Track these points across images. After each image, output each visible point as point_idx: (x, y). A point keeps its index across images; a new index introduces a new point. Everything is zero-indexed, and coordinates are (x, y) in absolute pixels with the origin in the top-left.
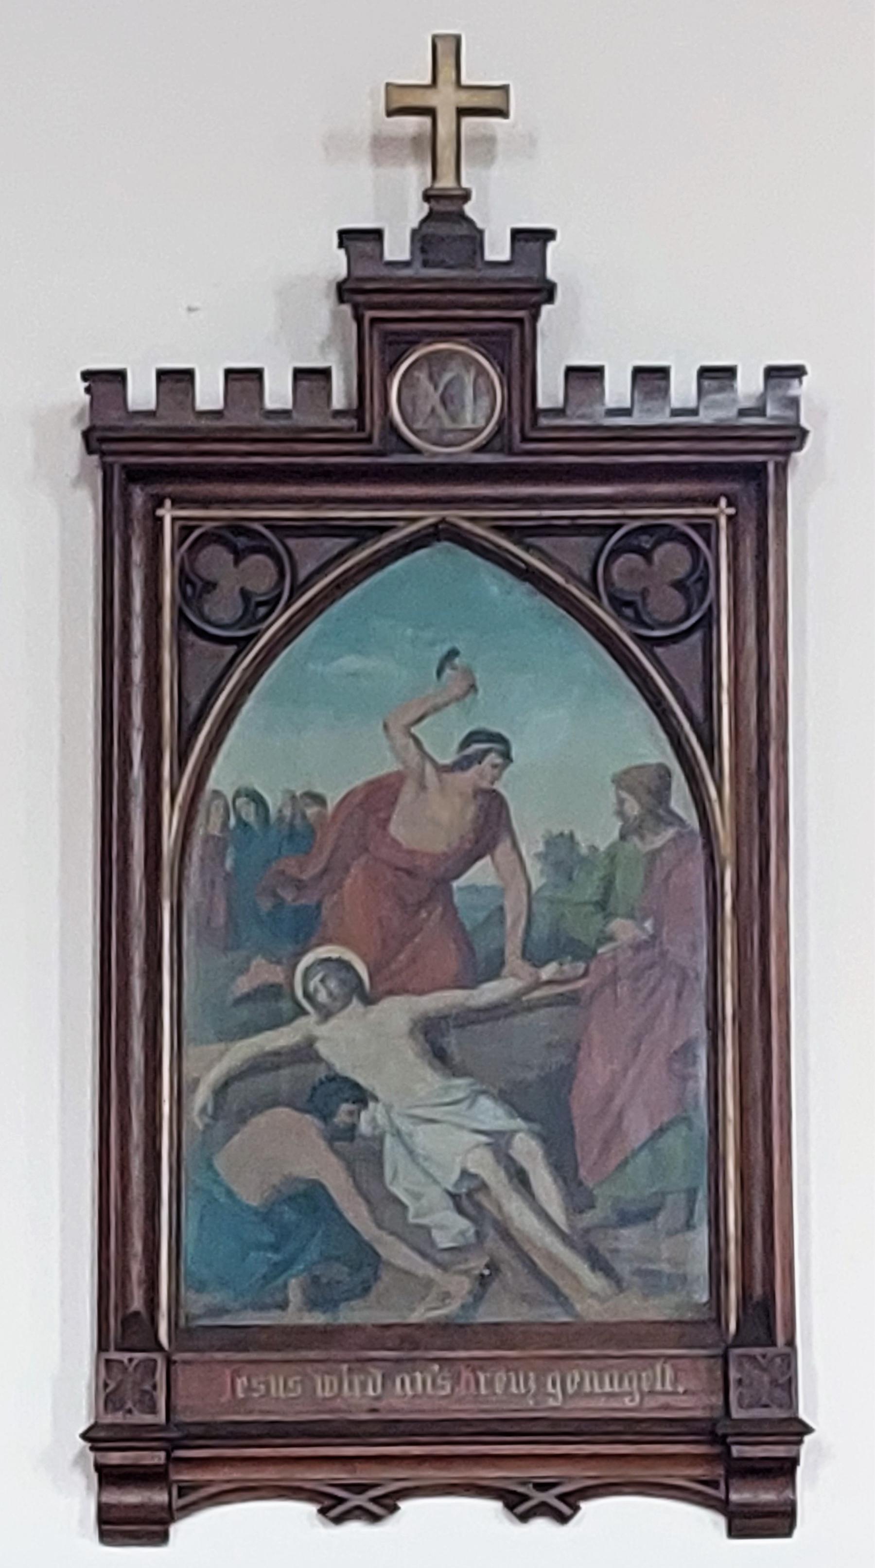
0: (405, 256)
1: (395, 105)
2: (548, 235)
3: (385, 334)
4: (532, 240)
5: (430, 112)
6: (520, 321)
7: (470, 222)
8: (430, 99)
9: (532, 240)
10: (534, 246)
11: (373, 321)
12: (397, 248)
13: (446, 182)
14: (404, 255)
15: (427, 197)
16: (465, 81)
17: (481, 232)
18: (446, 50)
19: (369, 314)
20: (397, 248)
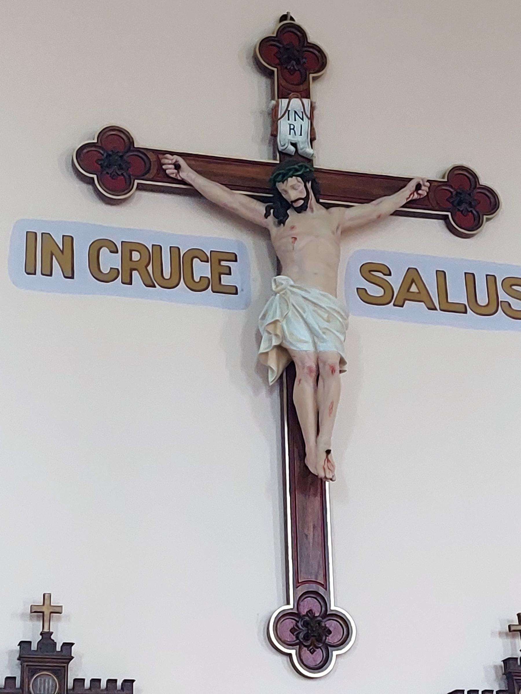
0: (36, 649)
1: (33, 611)
2: (72, 644)
3: (29, 669)
4: (68, 646)
5: (43, 612)
6: (64, 667)
7: (53, 640)
8: (44, 609)
9: (68, 646)
10: (68, 647)
11: (27, 665)
12: (34, 647)
13: (46, 630)
14: (36, 649)
15: (41, 634)
16: (52, 604)
17: (56, 643)
18: (46, 597)
19: (26, 664)
20: (34, 647)
